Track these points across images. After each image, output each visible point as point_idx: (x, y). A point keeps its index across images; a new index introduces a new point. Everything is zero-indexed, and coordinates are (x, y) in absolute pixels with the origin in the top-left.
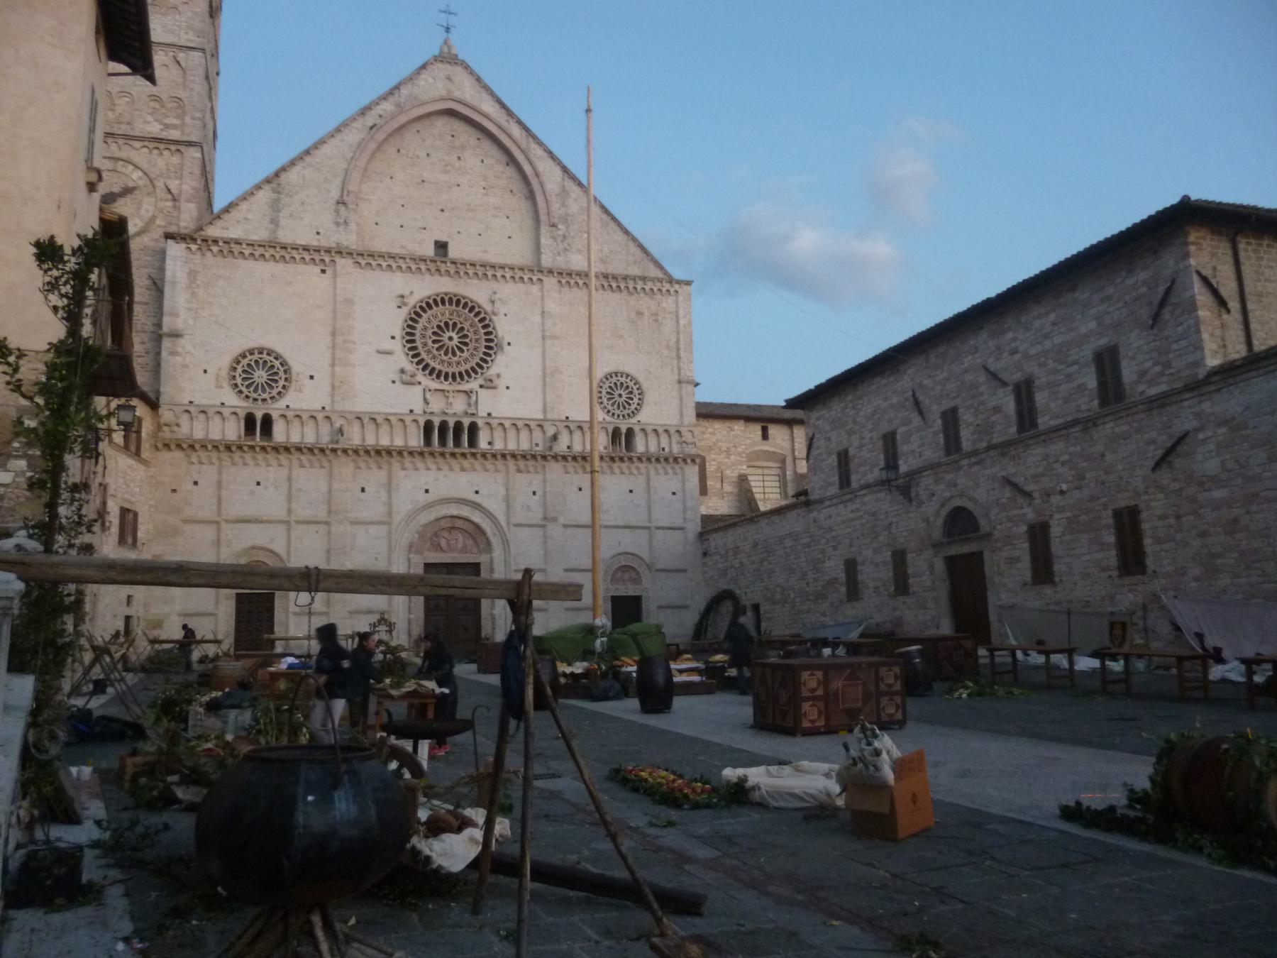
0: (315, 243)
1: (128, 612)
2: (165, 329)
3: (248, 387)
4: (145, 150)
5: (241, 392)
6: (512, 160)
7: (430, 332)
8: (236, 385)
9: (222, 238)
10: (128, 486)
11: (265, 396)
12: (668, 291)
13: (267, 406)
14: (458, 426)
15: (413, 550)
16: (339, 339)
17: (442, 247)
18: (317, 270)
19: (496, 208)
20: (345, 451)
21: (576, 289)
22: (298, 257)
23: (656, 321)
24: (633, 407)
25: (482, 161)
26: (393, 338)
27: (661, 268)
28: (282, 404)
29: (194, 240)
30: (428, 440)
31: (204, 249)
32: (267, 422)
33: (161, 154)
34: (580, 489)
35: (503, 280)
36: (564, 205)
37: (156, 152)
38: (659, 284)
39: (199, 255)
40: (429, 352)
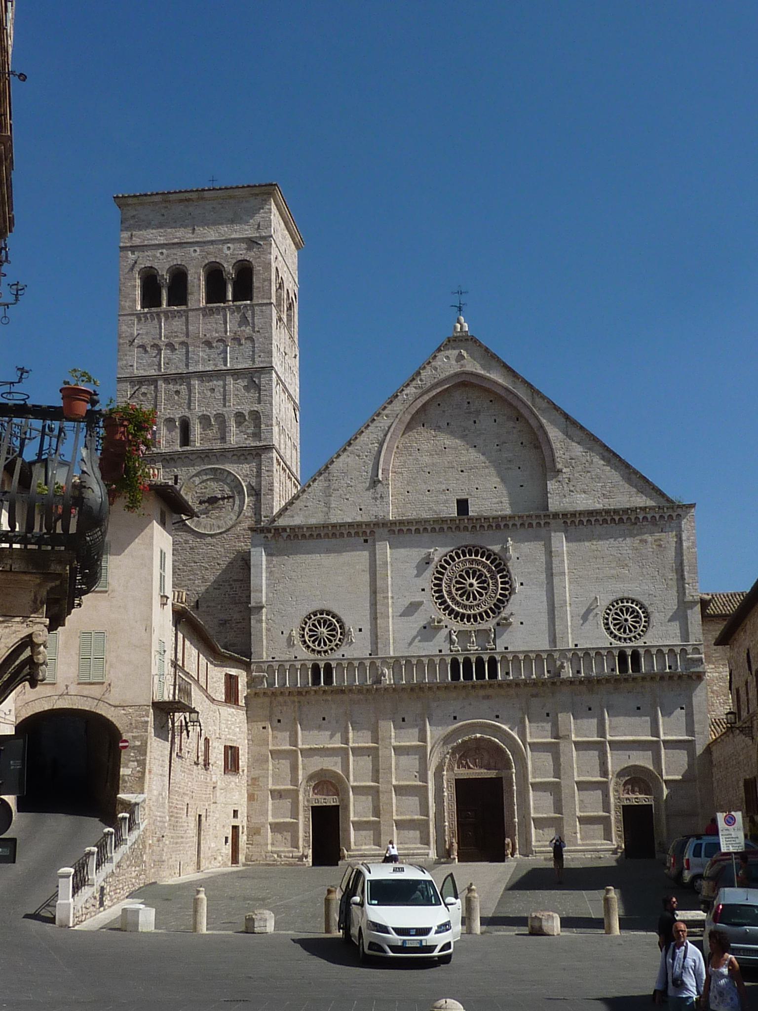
0: (359, 519)
1: (236, 822)
2: (253, 604)
3: (314, 642)
4: (235, 457)
5: (308, 647)
6: (519, 417)
7: (454, 581)
8: (305, 642)
9: (288, 526)
10: (230, 728)
11: (326, 648)
12: (670, 516)
13: (327, 657)
14: (480, 661)
15: (445, 768)
16: (379, 596)
17: (463, 505)
18: (362, 539)
19: (510, 461)
20: (386, 689)
21: (581, 526)
22: (345, 532)
23: (660, 546)
24: (639, 631)
25: (495, 421)
26: (423, 590)
27: (662, 495)
28: (338, 654)
29: (269, 531)
30: (455, 676)
31: (276, 535)
32: (328, 668)
33: (246, 459)
34: (590, 709)
35: (515, 527)
36: (567, 449)
37: (242, 458)
38: (661, 511)
39: (274, 542)
40: (453, 599)
